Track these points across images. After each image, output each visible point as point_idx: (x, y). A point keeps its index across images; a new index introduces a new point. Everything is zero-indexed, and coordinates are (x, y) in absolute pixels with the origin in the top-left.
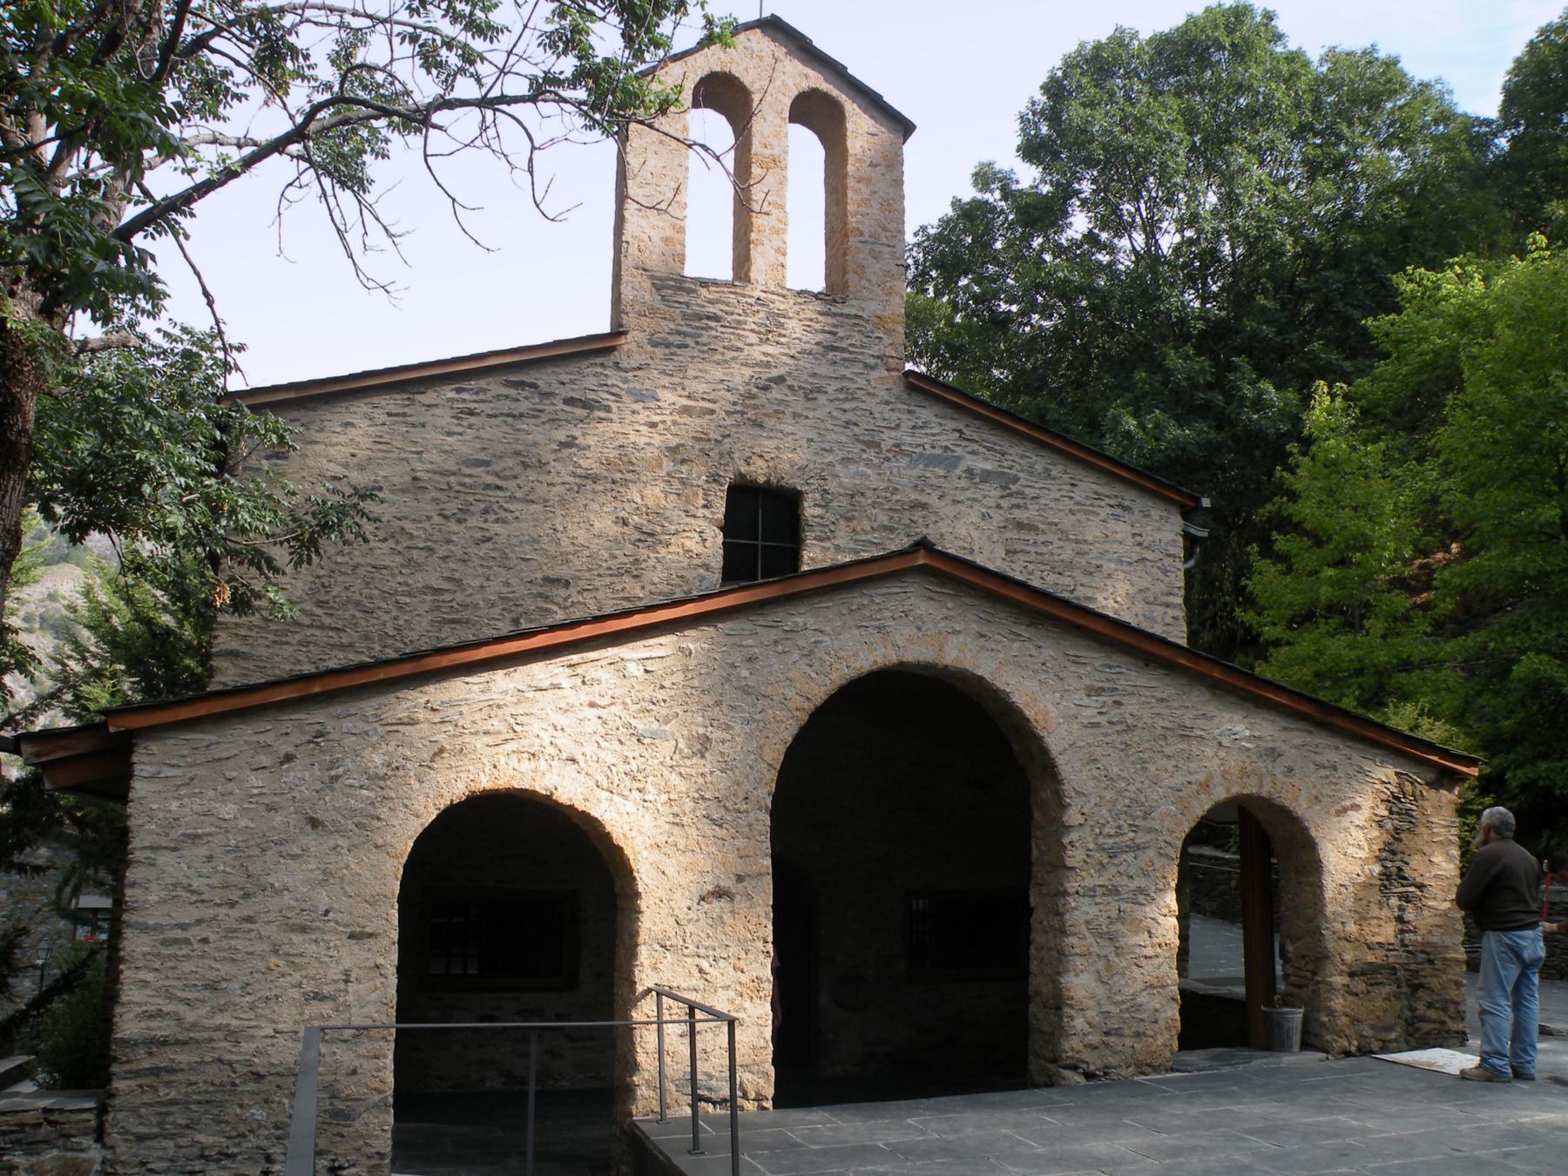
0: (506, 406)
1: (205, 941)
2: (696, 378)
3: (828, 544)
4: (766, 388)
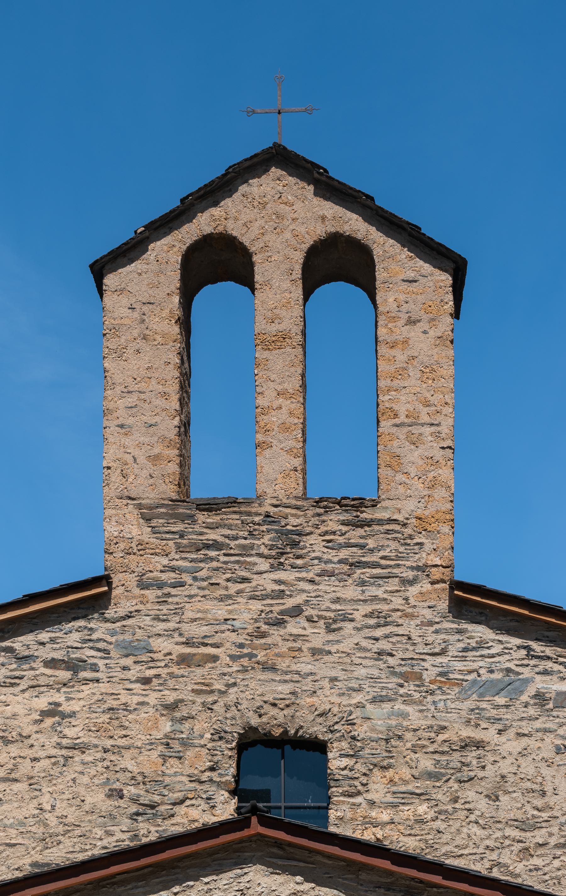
2: (195, 620)
3: (359, 800)
4: (279, 623)
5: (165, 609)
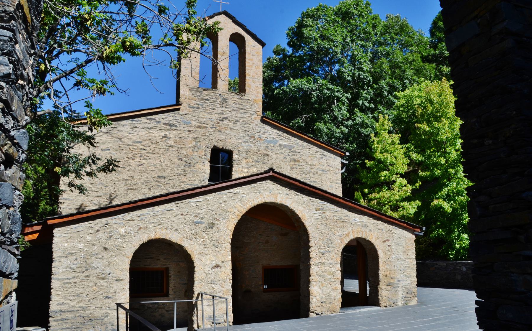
0: (146, 125)
1: (75, 283)
3: (240, 166)
4: (222, 121)
5: (195, 113)
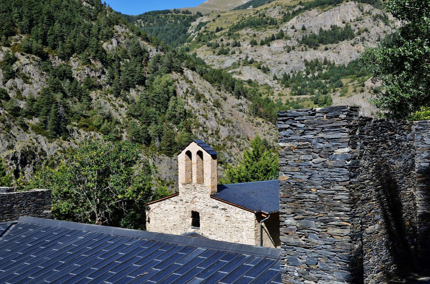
0: (168, 203)
